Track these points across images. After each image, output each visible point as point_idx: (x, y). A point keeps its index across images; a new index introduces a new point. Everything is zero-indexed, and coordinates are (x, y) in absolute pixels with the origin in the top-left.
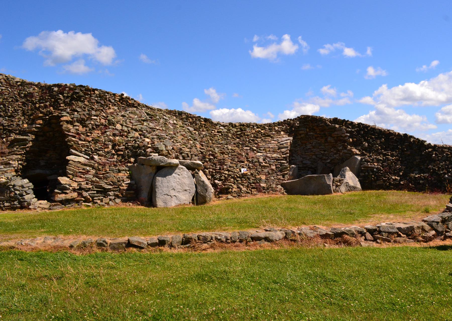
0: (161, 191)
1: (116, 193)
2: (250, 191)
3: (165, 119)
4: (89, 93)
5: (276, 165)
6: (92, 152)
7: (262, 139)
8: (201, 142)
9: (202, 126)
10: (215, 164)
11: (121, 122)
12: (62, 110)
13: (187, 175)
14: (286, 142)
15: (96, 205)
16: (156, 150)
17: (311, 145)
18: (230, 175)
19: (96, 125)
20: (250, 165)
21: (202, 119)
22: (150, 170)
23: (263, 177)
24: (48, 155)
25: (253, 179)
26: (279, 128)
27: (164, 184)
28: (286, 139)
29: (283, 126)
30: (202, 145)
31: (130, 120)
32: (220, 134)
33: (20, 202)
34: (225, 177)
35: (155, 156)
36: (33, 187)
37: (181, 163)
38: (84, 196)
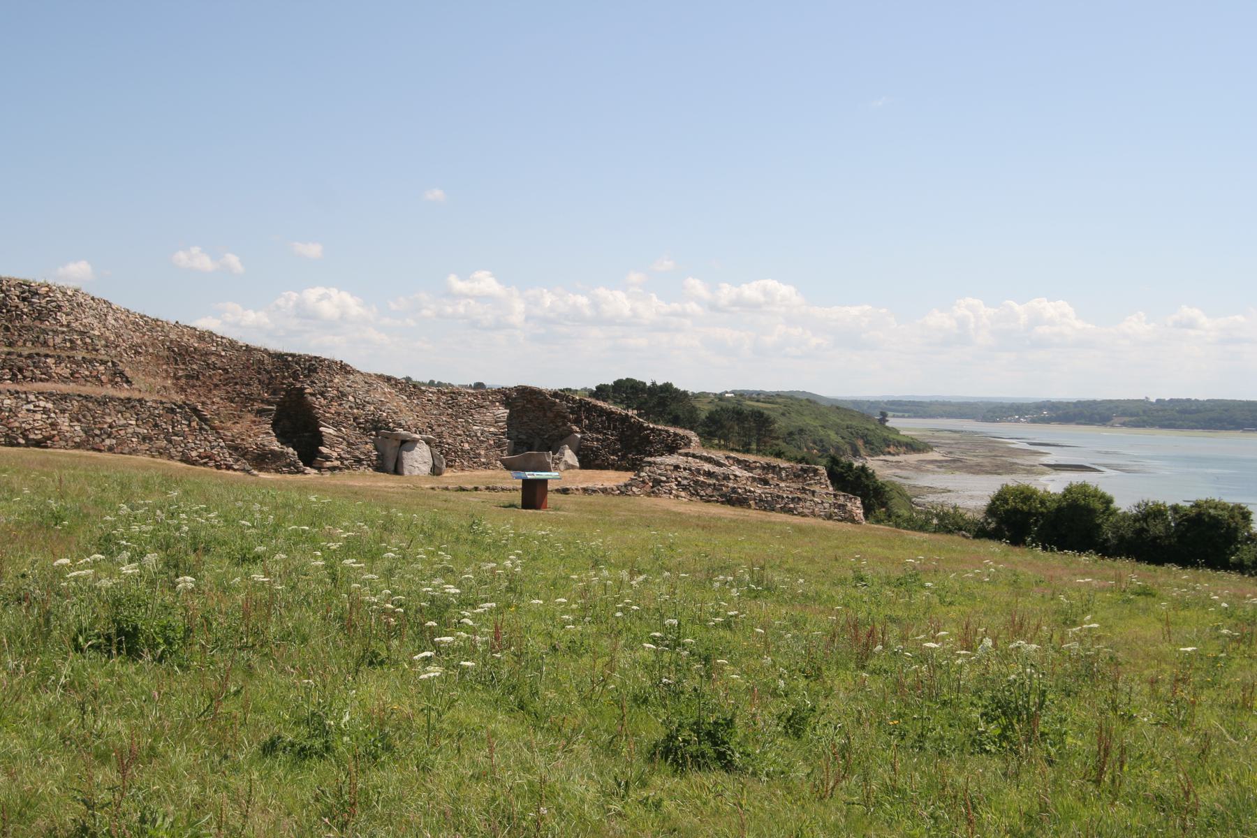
16: (400, 425)
22: (397, 444)
23: (483, 453)
28: (503, 412)
35: (400, 431)
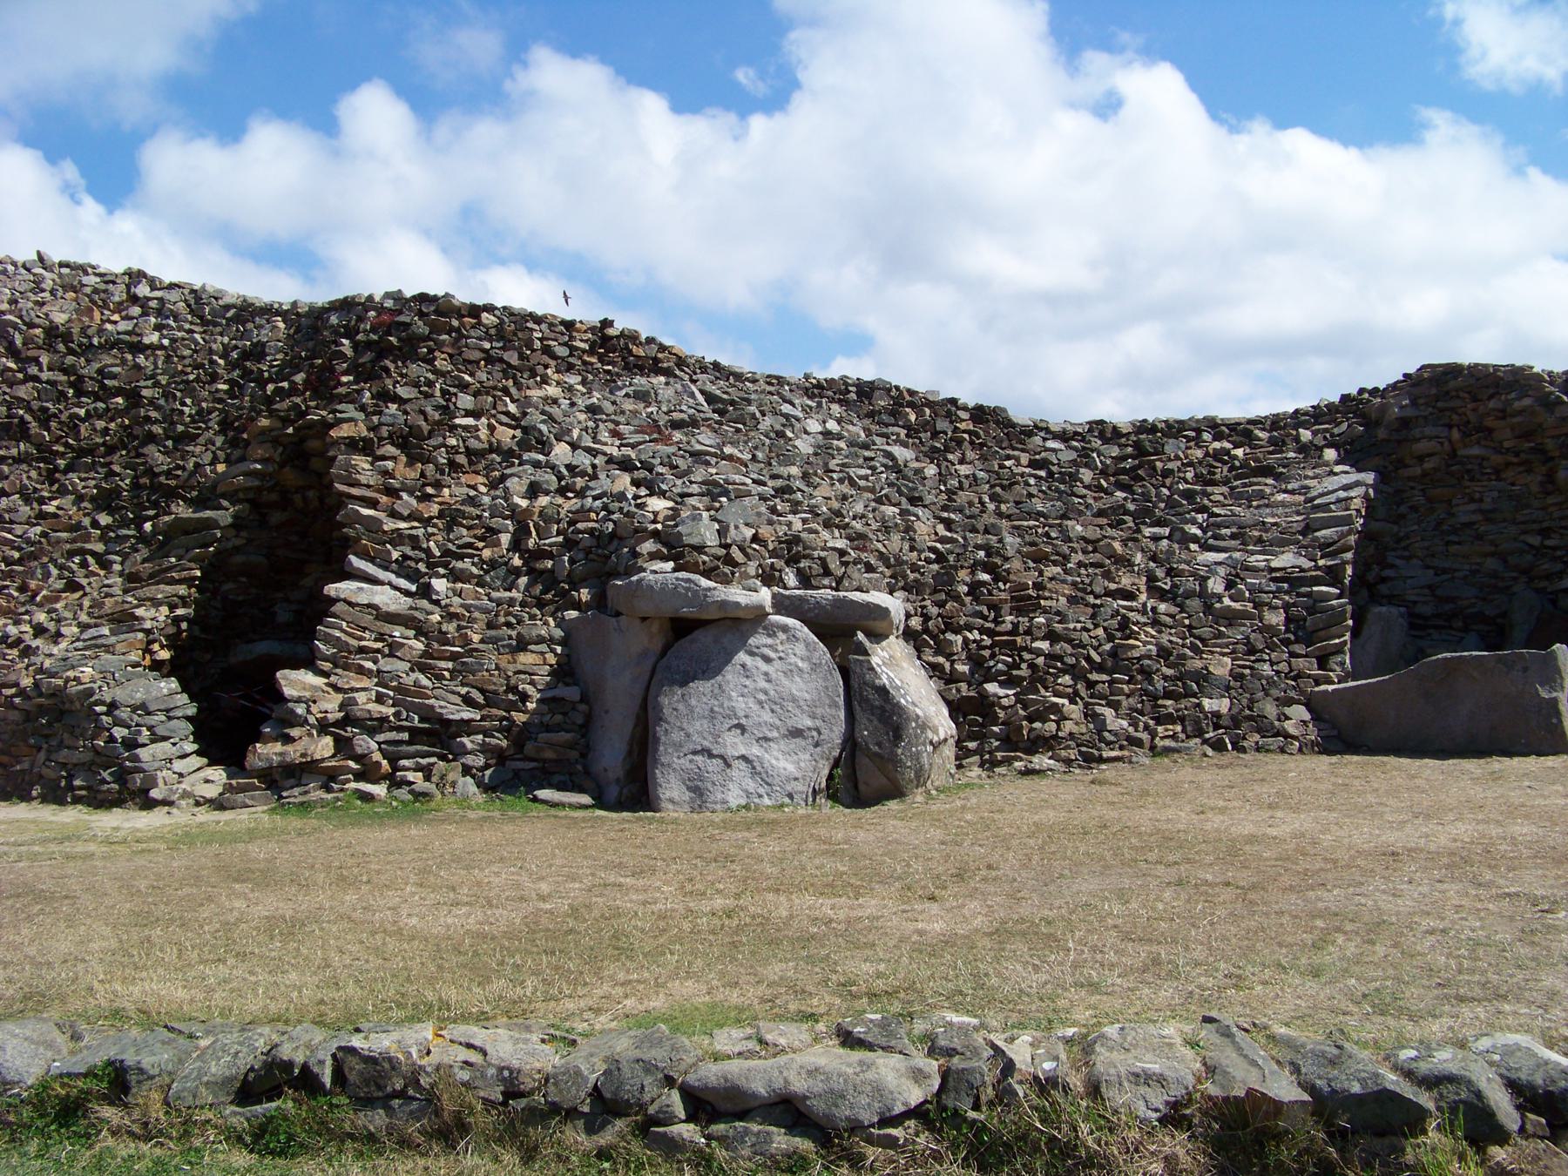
0: (676, 736)
1: (494, 741)
2: (1145, 736)
3: (787, 416)
4: (455, 323)
5: (1286, 607)
6: (430, 566)
7: (1232, 489)
8: (945, 508)
9: (960, 442)
10: (993, 607)
11: (576, 433)
12: (343, 399)
13: (809, 659)
14: (1342, 494)
15: (403, 793)
16: (674, 548)
17: (1473, 507)
18: (1059, 658)
19: (469, 452)
20: (1162, 607)
21: (965, 408)
25: (1165, 678)
26: (1314, 433)
27: (693, 702)
28: (1344, 485)
29: (1338, 424)
30: (948, 524)
31: (617, 423)
32: (1043, 473)
33: (122, 776)
34: (1032, 666)
35: (660, 572)
36: (192, 710)
37: (781, 605)
38: (359, 751)
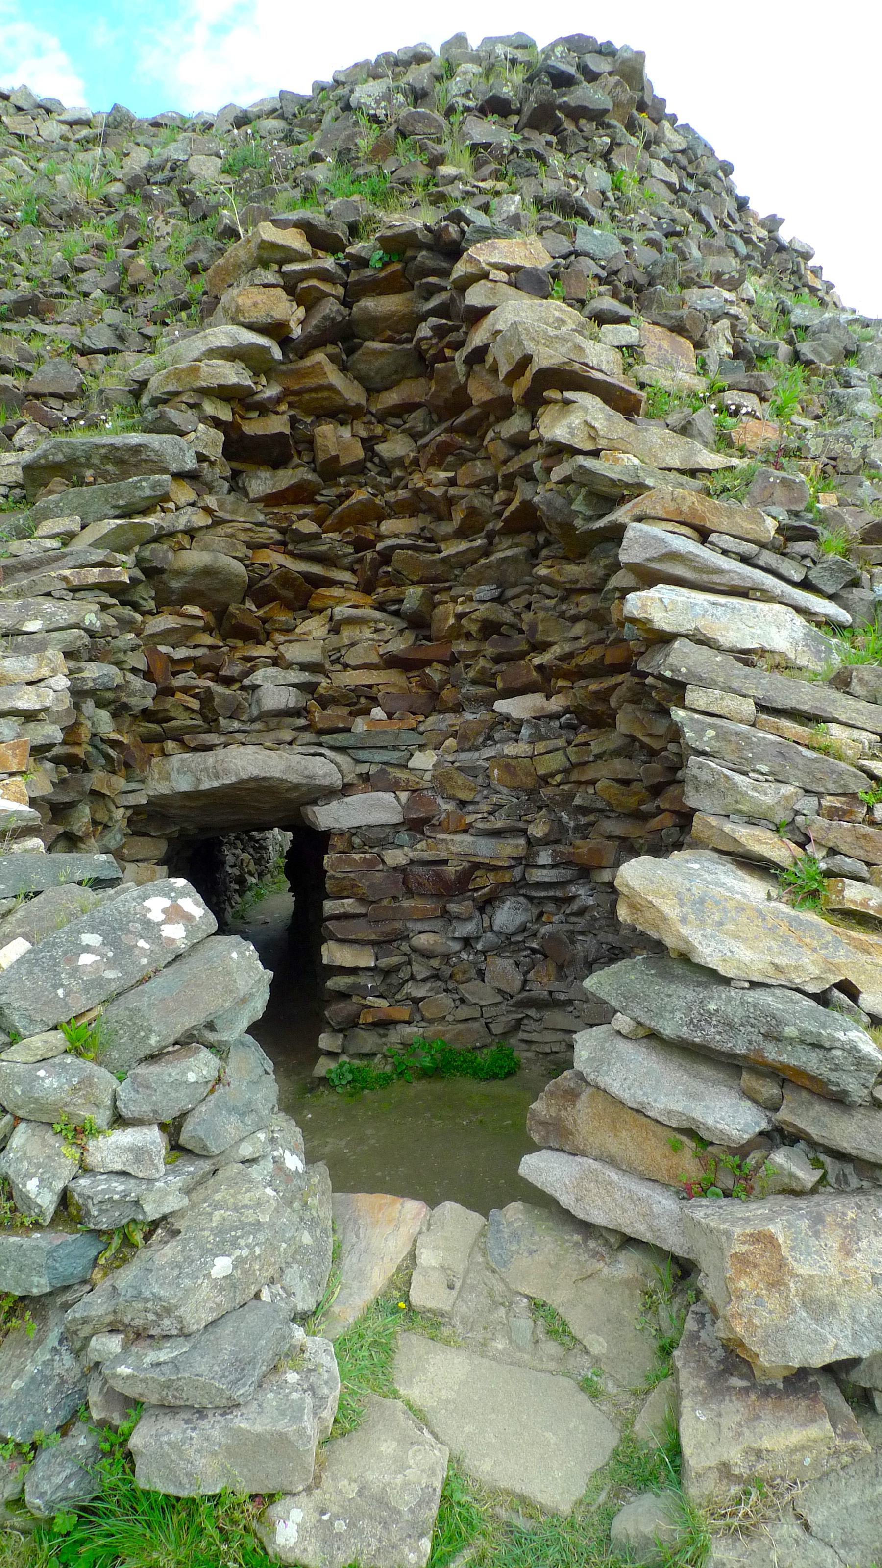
24: (315, 627)
